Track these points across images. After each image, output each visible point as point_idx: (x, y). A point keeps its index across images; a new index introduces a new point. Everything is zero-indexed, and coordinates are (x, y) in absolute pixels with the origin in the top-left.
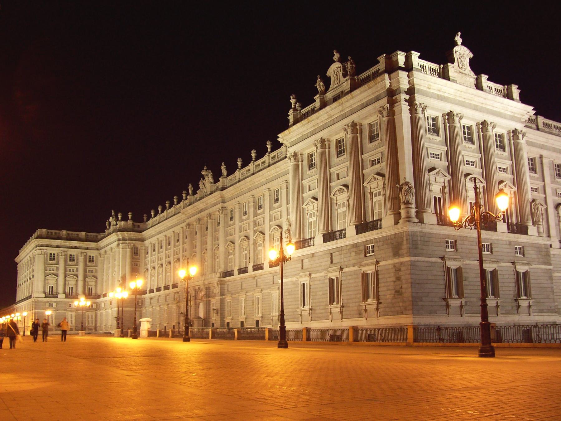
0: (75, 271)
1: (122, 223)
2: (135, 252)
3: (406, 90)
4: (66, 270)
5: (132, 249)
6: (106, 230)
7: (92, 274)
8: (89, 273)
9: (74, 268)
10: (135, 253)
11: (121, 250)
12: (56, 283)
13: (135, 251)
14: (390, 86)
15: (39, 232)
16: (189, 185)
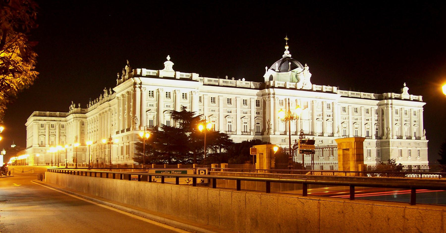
0: (54, 133)
1: (76, 109)
2: (83, 124)
3: (140, 83)
4: (49, 132)
5: (81, 122)
6: (69, 112)
7: (63, 134)
8: (62, 134)
9: (54, 131)
10: (82, 124)
11: (75, 123)
12: (44, 139)
13: (82, 123)
14: (135, 81)
15: (35, 113)
16: (100, 95)
